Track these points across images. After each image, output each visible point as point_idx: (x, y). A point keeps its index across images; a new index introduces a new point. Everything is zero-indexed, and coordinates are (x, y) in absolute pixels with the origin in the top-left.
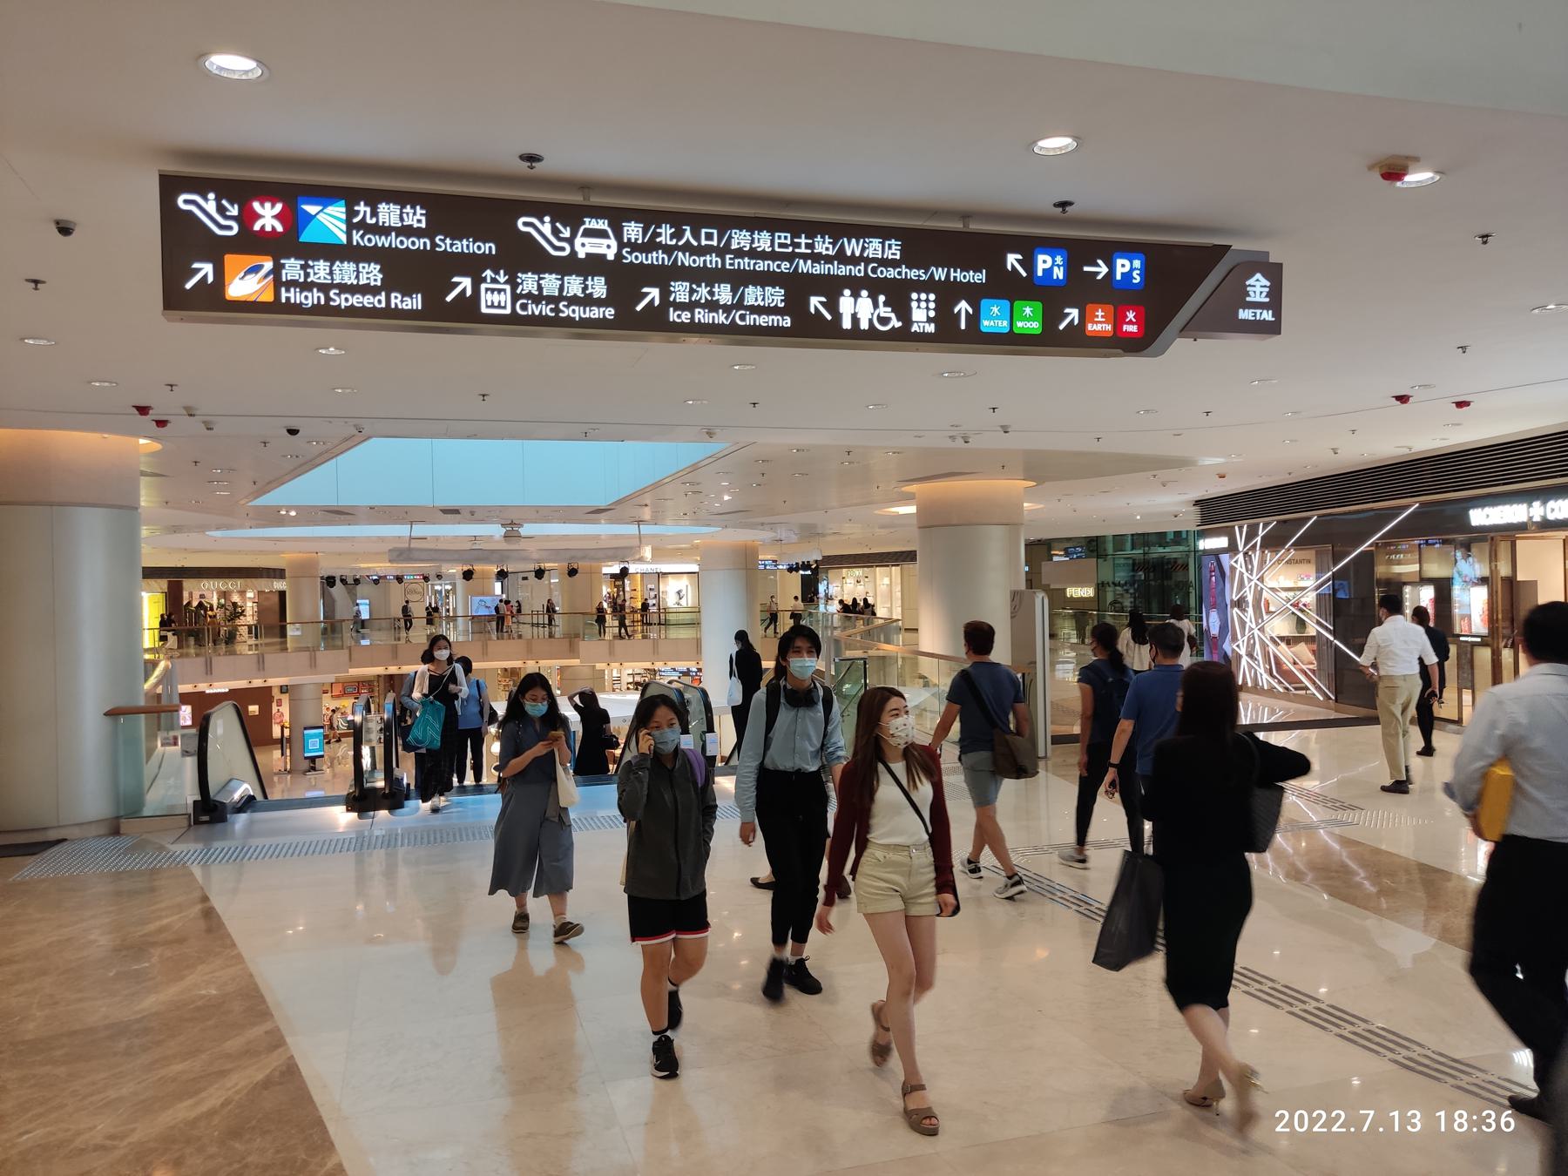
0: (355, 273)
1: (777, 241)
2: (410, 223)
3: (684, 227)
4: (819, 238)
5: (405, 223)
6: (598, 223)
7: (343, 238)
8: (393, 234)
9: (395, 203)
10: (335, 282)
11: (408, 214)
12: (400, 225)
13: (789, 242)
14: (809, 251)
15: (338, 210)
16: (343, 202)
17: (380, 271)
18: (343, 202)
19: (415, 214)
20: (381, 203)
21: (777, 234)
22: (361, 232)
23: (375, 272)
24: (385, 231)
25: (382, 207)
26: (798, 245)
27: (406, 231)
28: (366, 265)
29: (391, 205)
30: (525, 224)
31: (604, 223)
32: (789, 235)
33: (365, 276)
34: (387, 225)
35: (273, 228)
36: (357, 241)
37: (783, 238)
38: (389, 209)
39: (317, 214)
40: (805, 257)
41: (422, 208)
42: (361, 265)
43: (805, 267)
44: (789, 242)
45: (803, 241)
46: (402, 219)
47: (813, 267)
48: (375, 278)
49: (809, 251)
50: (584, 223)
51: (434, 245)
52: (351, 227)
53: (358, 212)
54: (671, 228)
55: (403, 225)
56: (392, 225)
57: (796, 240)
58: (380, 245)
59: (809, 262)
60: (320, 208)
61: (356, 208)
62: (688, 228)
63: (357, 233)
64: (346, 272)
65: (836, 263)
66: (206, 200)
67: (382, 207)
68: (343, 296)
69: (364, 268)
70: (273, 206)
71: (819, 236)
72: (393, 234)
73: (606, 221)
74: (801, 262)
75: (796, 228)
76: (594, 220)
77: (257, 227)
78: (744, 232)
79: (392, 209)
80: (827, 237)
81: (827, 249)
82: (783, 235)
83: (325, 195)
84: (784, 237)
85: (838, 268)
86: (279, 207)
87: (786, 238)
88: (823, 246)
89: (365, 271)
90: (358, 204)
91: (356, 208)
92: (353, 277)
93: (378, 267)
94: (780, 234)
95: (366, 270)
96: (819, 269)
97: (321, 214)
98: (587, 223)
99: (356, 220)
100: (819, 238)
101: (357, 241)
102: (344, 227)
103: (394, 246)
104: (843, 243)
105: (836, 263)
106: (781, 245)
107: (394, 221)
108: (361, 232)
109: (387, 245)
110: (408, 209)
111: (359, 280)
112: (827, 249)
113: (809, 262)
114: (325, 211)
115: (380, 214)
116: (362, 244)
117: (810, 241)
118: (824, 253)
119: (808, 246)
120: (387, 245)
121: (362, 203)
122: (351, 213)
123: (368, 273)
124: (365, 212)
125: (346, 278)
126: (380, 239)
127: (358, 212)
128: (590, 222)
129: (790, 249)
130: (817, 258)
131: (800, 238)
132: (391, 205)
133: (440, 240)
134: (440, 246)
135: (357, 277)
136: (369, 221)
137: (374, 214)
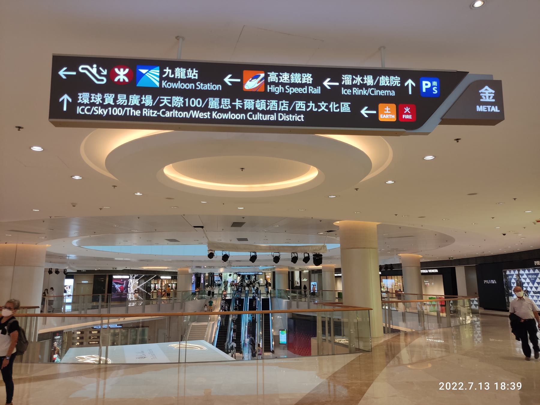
2: (190, 76)
5: (188, 77)
12: (185, 78)
15: (156, 72)
16: (158, 68)
18: (158, 68)
19: (193, 72)
20: (176, 68)
22: (166, 81)
24: (175, 80)
25: (177, 70)
27: (188, 80)
29: (181, 68)
34: (179, 78)
35: (124, 80)
36: (164, 85)
38: (180, 70)
39: (146, 73)
41: (196, 70)
46: (186, 75)
52: (161, 79)
53: (165, 72)
55: (186, 78)
56: (182, 78)
60: (147, 70)
61: (165, 70)
63: (164, 82)
66: (92, 67)
67: (177, 70)
70: (124, 70)
79: (182, 71)
83: (150, 64)
90: (166, 69)
91: (165, 70)
97: (148, 73)
99: (164, 76)
101: (164, 85)
102: (158, 79)
107: (183, 76)
108: (166, 81)
110: (190, 70)
114: (150, 72)
115: (176, 73)
121: (167, 68)
122: (162, 73)
124: (169, 72)
127: (165, 72)
136: (170, 76)
137: (173, 73)
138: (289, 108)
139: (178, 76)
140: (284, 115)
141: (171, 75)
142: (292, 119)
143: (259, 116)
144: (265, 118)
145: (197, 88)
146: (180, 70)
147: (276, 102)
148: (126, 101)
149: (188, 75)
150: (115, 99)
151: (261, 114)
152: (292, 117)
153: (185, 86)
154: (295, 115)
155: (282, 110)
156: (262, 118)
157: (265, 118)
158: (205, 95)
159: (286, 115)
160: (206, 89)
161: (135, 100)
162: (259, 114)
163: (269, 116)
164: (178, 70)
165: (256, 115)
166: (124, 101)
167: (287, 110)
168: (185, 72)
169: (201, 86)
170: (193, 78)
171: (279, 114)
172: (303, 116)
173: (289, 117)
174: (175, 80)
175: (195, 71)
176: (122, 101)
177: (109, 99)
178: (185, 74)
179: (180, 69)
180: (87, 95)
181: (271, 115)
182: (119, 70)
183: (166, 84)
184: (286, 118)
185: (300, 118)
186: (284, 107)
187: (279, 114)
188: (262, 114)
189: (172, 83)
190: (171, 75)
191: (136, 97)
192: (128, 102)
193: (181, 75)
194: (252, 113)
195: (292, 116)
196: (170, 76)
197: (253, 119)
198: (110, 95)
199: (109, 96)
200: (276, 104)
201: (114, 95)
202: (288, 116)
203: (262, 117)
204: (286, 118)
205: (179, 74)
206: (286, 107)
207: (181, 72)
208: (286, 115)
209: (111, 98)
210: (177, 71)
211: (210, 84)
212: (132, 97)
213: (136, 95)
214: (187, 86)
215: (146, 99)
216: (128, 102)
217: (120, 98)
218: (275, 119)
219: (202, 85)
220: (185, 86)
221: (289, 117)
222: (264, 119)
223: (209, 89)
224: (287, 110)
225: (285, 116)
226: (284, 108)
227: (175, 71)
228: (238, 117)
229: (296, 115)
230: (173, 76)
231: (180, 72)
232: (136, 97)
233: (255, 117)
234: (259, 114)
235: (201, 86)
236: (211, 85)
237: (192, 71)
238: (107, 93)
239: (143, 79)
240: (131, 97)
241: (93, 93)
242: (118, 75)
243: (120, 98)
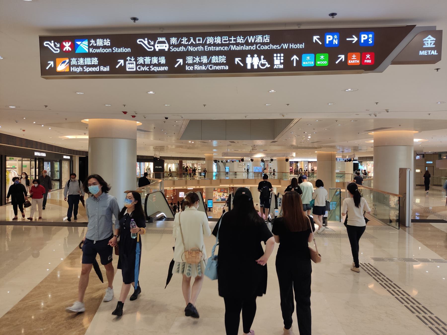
0: (91, 61)
1: (223, 39)
2: (106, 44)
3: (191, 38)
4: (238, 37)
5: (104, 45)
7: (87, 51)
8: (101, 48)
9: (101, 39)
10: (85, 64)
11: (105, 41)
12: (103, 45)
13: (227, 39)
14: (235, 42)
17: (97, 60)
19: (107, 41)
20: (97, 39)
21: (223, 37)
22: (92, 48)
23: (96, 60)
24: (98, 47)
26: (231, 40)
28: (94, 58)
29: (100, 39)
32: (227, 37)
33: (93, 62)
34: (99, 45)
37: (225, 38)
38: (100, 41)
40: (233, 44)
41: (109, 39)
42: (92, 59)
43: (233, 48)
44: (227, 39)
45: (233, 39)
46: (103, 43)
47: (236, 48)
48: (96, 62)
49: (235, 42)
52: (89, 47)
53: (91, 42)
54: (186, 38)
55: (104, 45)
56: (101, 45)
57: (230, 39)
58: (97, 52)
59: (235, 46)
61: (91, 41)
62: (192, 38)
63: (91, 49)
64: (88, 61)
65: (245, 45)
67: (98, 40)
68: (87, 68)
69: (93, 59)
71: (238, 36)
72: (101, 48)
74: (232, 46)
75: (229, 34)
78: (211, 38)
80: (241, 36)
81: (242, 41)
82: (225, 37)
84: (226, 38)
85: (246, 47)
87: (226, 38)
88: (240, 40)
89: (93, 60)
90: (91, 40)
91: (91, 41)
92: (90, 62)
93: (97, 59)
94: (224, 37)
95: (94, 60)
96: (239, 48)
99: (90, 45)
100: (238, 37)
102: (87, 47)
104: (247, 38)
105: (245, 45)
106: (224, 41)
107: (101, 44)
108: (92, 48)
109: (99, 52)
110: (105, 40)
111: (91, 63)
112: (242, 41)
113: (235, 46)
115: (97, 42)
116: (92, 52)
117: (235, 39)
118: (240, 42)
119: (234, 40)
120: (99, 52)
121: (92, 40)
122: (89, 43)
123: (94, 61)
124: (93, 42)
125: (88, 63)
126: (97, 50)
127: (91, 42)
129: (228, 42)
130: (237, 44)
131: (232, 38)
132: (100, 39)
135: (91, 62)
137: (96, 43)
141: (95, 44)
168: (102, 42)
174: (98, 47)
175: (108, 40)
189: (96, 50)
190: (95, 44)
205: (99, 43)
207: (100, 42)
210: (98, 41)
237: (106, 41)
239: (79, 47)
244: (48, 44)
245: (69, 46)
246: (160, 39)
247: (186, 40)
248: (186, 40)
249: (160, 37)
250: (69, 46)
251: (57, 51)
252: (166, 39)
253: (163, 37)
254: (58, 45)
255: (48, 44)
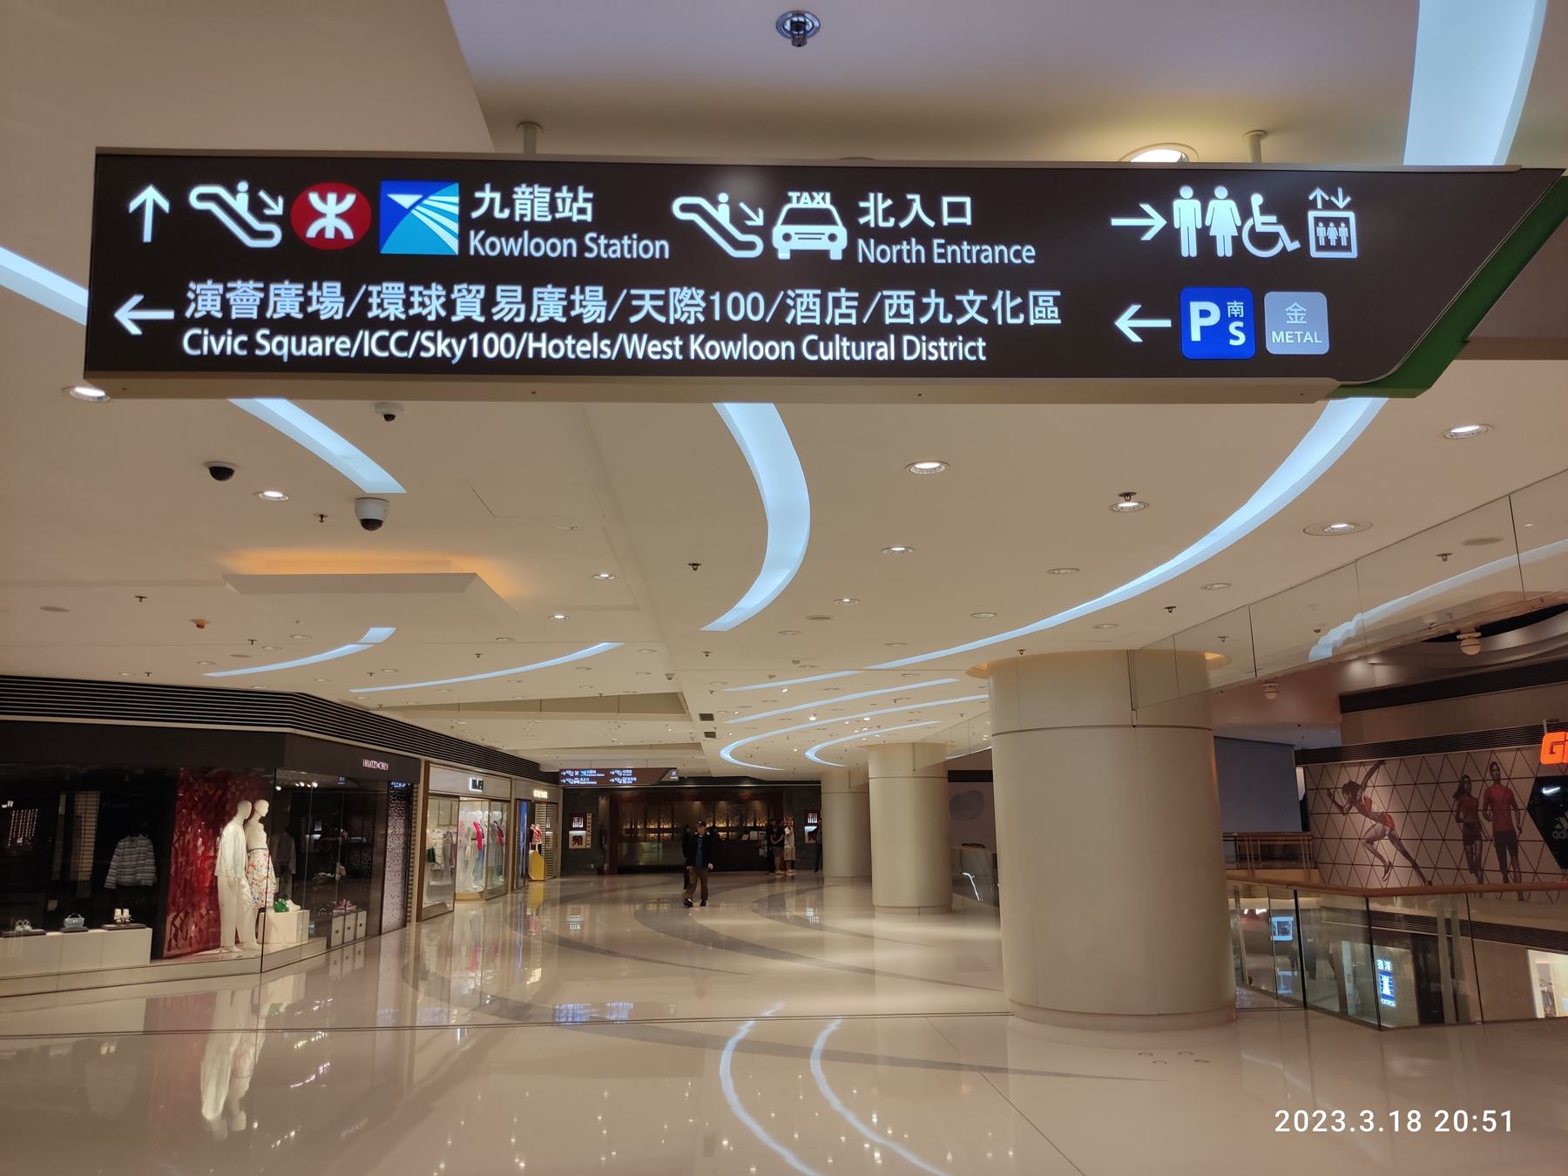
2: (567, 214)
3: (909, 197)
5: (558, 216)
6: (812, 198)
11: (564, 200)
12: (549, 218)
15: (447, 201)
16: (455, 187)
18: (455, 187)
19: (575, 199)
20: (519, 185)
22: (482, 233)
24: (511, 228)
25: (522, 193)
27: (561, 228)
29: (536, 186)
30: (685, 208)
31: (823, 198)
34: (527, 219)
38: (531, 193)
39: (413, 206)
41: (586, 191)
46: (553, 207)
50: (789, 200)
51: (583, 248)
52: (466, 224)
53: (481, 201)
54: (884, 199)
55: (554, 218)
56: (537, 219)
60: (416, 198)
61: (478, 195)
62: (917, 197)
67: (522, 193)
72: (526, 233)
73: (828, 195)
76: (806, 195)
77: (312, 232)
79: (536, 194)
86: (350, 199)
90: (482, 189)
91: (478, 195)
97: (418, 207)
98: (794, 200)
99: (475, 215)
102: (455, 227)
103: (526, 254)
107: (542, 214)
108: (482, 233)
110: (565, 193)
114: (425, 202)
115: (517, 202)
121: (488, 187)
122: (468, 203)
124: (492, 201)
127: (481, 201)
128: (799, 199)
133: (592, 239)
134: (591, 250)
136: (497, 214)
137: (508, 202)
138: (860, 316)
139: (523, 212)
140: (921, 341)
141: (501, 210)
142: (947, 353)
143: (841, 348)
144: (858, 352)
145: (587, 255)
146: (531, 193)
147: (815, 296)
148: (523, 307)
149: (560, 208)
150: (488, 303)
151: (845, 339)
152: (947, 349)
153: (545, 247)
154: (958, 341)
155: (838, 321)
156: (849, 353)
157: (858, 352)
158: (616, 277)
159: (927, 342)
160: (618, 255)
161: (551, 303)
162: (841, 340)
163: (871, 345)
164: (523, 193)
165: (831, 344)
166: (515, 307)
167: (853, 321)
168: (547, 199)
169: (601, 247)
170: (576, 218)
171: (906, 338)
172: (984, 344)
173: (937, 348)
174: (511, 228)
175: (582, 194)
176: (510, 310)
177: (469, 302)
178: (547, 205)
179: (531, 190)
180: (396, 291)
181: (879, 344)
182: (324, 199)
183: (482, 241)
184: (929, 353)
185: (973, 351)
186: (844, 310)
187: (906, 338)
188: (848, 340)
189: (503, 240)
190: (501, 210)
191: (553, 293)
192: (529, 312)
193: (536, 209)
194: (815, 337)
195: (946, 344)
196: (497, 214)
197: (820, 358)
198: (471, 287)
199: (469, 291)
200: (814, 303)
201: (482, 288)
202: (935, 344)
203: (849, 348)
204: (929, 353)
205: (529, 207)
206: (849, 311)
207: (536, 200)
208: (927, 342)
209: (475, 297)
211: (630, 238)
212: (543, 293)
213: (555, 285)
214: (554, 248)
215: (584, 300)
216: (529, 312)
217: (502, 297)
218: (893, 358)
219: (603, 241)
220: (545, 247)
221: (937, 348)
222: (856, 358)
223: (627, 256)
224: (853, 321)
225: (924, 344)
226: (842, 316)
227: (515, 196)
228: (772, 350)
229: (960, 338)
230: (506, 213)
231: (532, 201)
232: (553, 293)
233: (826, 352)
234: (841, 340)
235: (598, 245)
236: (635, 243)
237: (571, 195)
238: (461, 282)
240: (539, 293)
241: (417, 283)
242: (319, 215)
243: (502, 297)
244: (215, 198)
245: (339, 216)
246: (801, 200)
247: (882, 206)
248: (885, 211)
249: (801, 189)
250: (339, 216)
251: (268, 235)
252: (833, 202)
253: (818, 190)
254: (277, 208)
255: (215, 198)
